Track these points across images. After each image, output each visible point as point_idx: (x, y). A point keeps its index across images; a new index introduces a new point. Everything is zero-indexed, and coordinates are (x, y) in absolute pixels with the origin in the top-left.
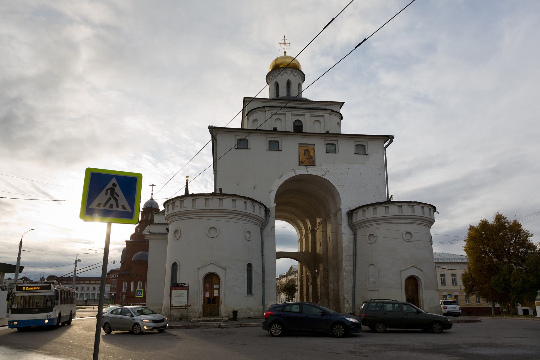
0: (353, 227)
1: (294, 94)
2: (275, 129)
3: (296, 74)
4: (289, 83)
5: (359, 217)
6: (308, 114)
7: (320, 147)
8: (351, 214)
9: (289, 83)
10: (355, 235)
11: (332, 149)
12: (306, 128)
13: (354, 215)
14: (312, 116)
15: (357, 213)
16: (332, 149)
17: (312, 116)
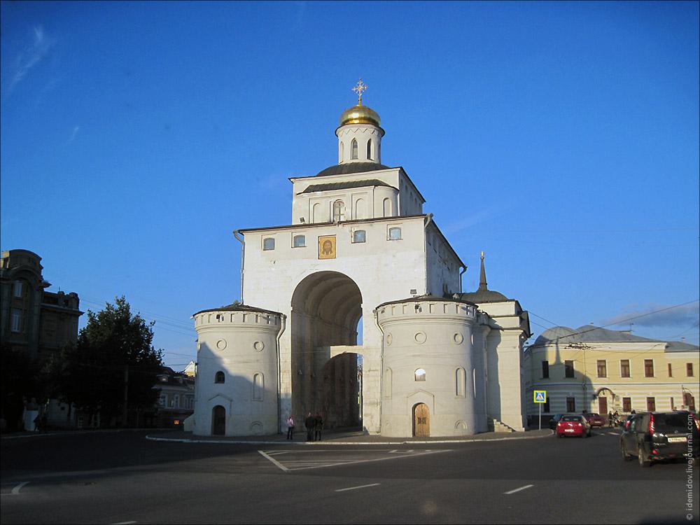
1: (362, 158)
6: (348, 192)
16: (359, 238)
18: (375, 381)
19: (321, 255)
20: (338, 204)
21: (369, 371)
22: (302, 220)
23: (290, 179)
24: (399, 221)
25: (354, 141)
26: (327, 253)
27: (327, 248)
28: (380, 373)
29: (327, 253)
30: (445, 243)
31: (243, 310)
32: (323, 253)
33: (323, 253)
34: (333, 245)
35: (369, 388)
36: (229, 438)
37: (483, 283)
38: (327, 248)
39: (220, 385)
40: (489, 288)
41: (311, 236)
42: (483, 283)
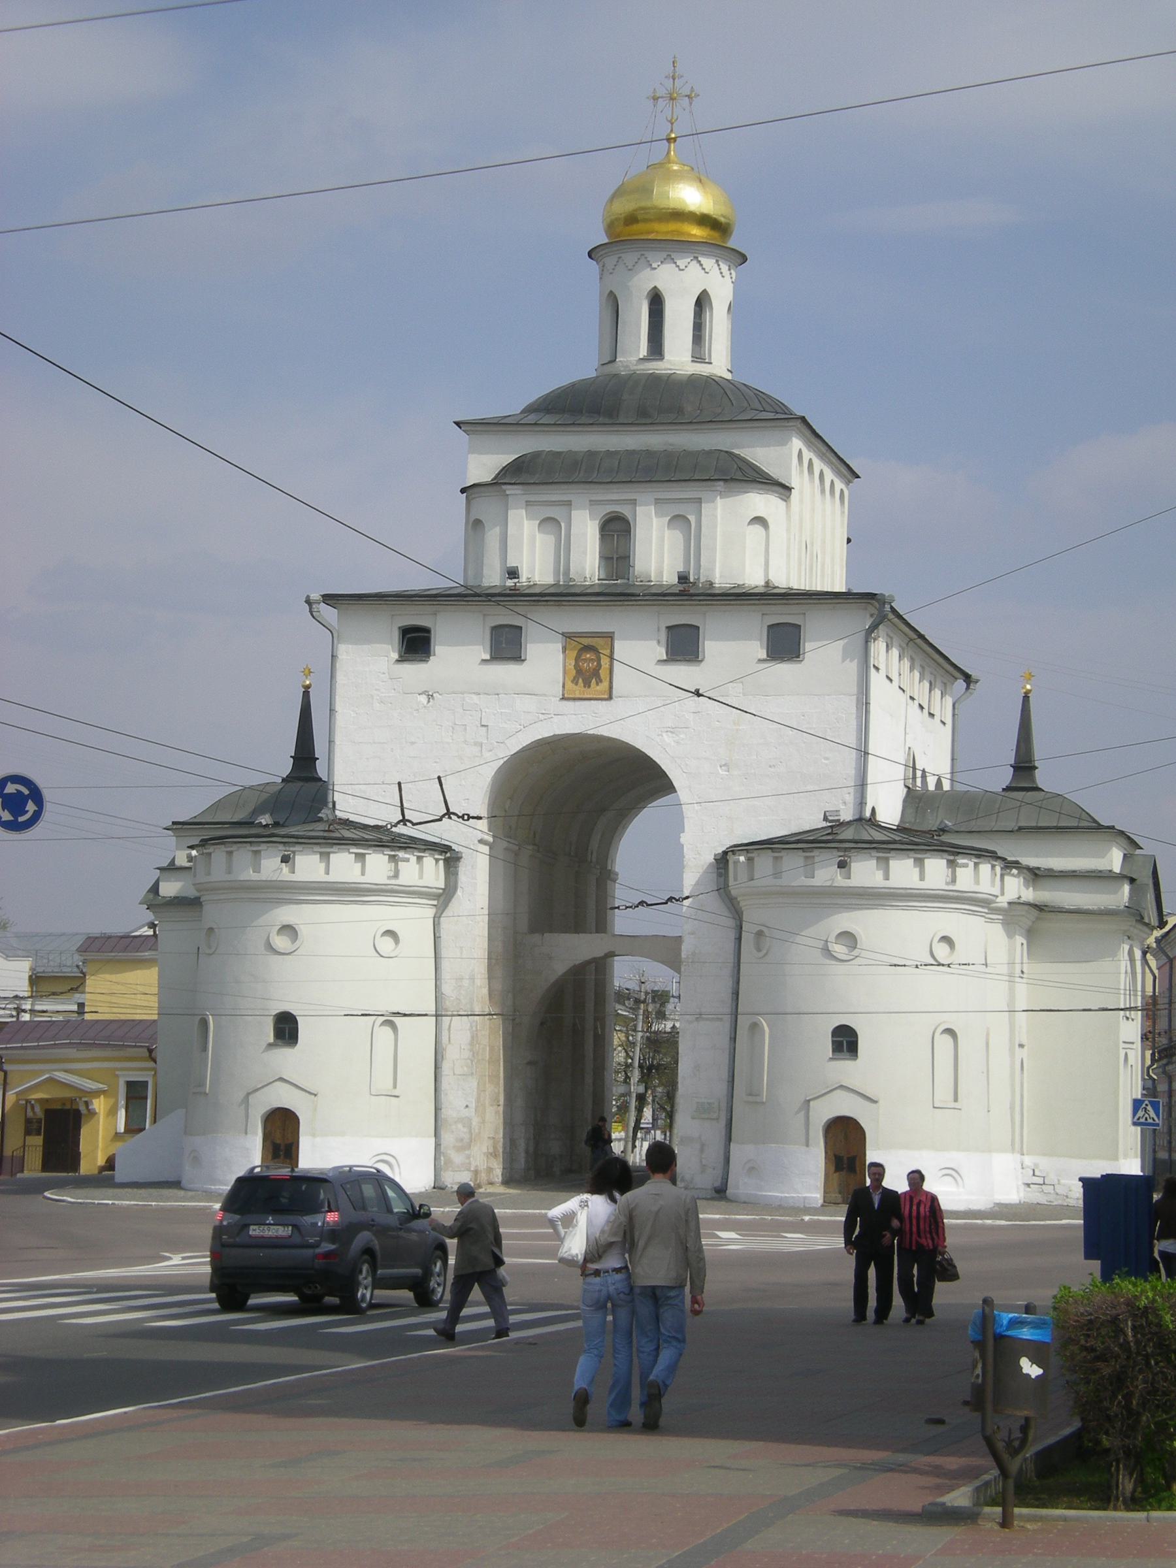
1: (678, 358)
8: (722, 860)
11: (683, 646)
16: (683, 646)
22: (513, 573)
23: (458, 424)
25: (656, 302)
26: (587, 684)
27: (590, 669)
29: (587, 684)
30: (919, 641)
31: (355, 842)
32: (575, 681)
34: (605, 662)
37: (1024, 767)
38: (590, 669)
40: (1043, 777)
42: (1024, 767)
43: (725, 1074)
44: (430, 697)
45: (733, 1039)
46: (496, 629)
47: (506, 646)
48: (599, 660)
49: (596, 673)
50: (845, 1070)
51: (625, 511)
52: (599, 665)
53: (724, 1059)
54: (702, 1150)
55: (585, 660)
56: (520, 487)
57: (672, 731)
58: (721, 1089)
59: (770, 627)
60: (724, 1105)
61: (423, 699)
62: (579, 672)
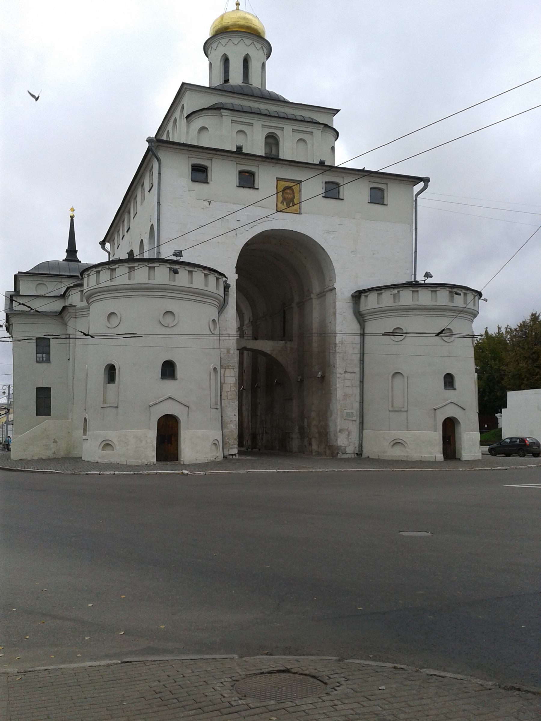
0: (361, 317)
2: (240, 148)
3: (259, 46)
4: (246, 61)
5: (370, 303)
6: (288, 128)
7: (312, 187)
8: (358, 296)
9: (246, 61)
10: (363, 328)
12: (287, 151)
13: (363, 298)
14: (294, 130)
15: (367, 296)
16: (332, 192)
17: (294, 130)
18: (352, 386)
19: (279, 205)
20: (272, 140)
21: (346, 372)
24: (384, 181)
27: (288, 197)
28: (358, 376)
32: (282, 202)
33: (282, 202)
35: (346, 396)
36: (185, 466)
38: (288, 197)
39: (169, 383)
41: (267, 179)
43: (358, 398)
44: (210, 202)
45: (362, 382)
46: (241, 172)
47: (247, 180)
48: (294, 193)
49: (292, 200)
50: (450, 393)
51: (278, 133)
52: (294, 197)
53: (357, 391)
54: (349, 435)
55: (287, 193)
56: (229, 112)
57: (328, 232)
58: (357, 405)
59: (371, 188)
60: (358, 413)
61: (206, 203)
62: (284, 199)
